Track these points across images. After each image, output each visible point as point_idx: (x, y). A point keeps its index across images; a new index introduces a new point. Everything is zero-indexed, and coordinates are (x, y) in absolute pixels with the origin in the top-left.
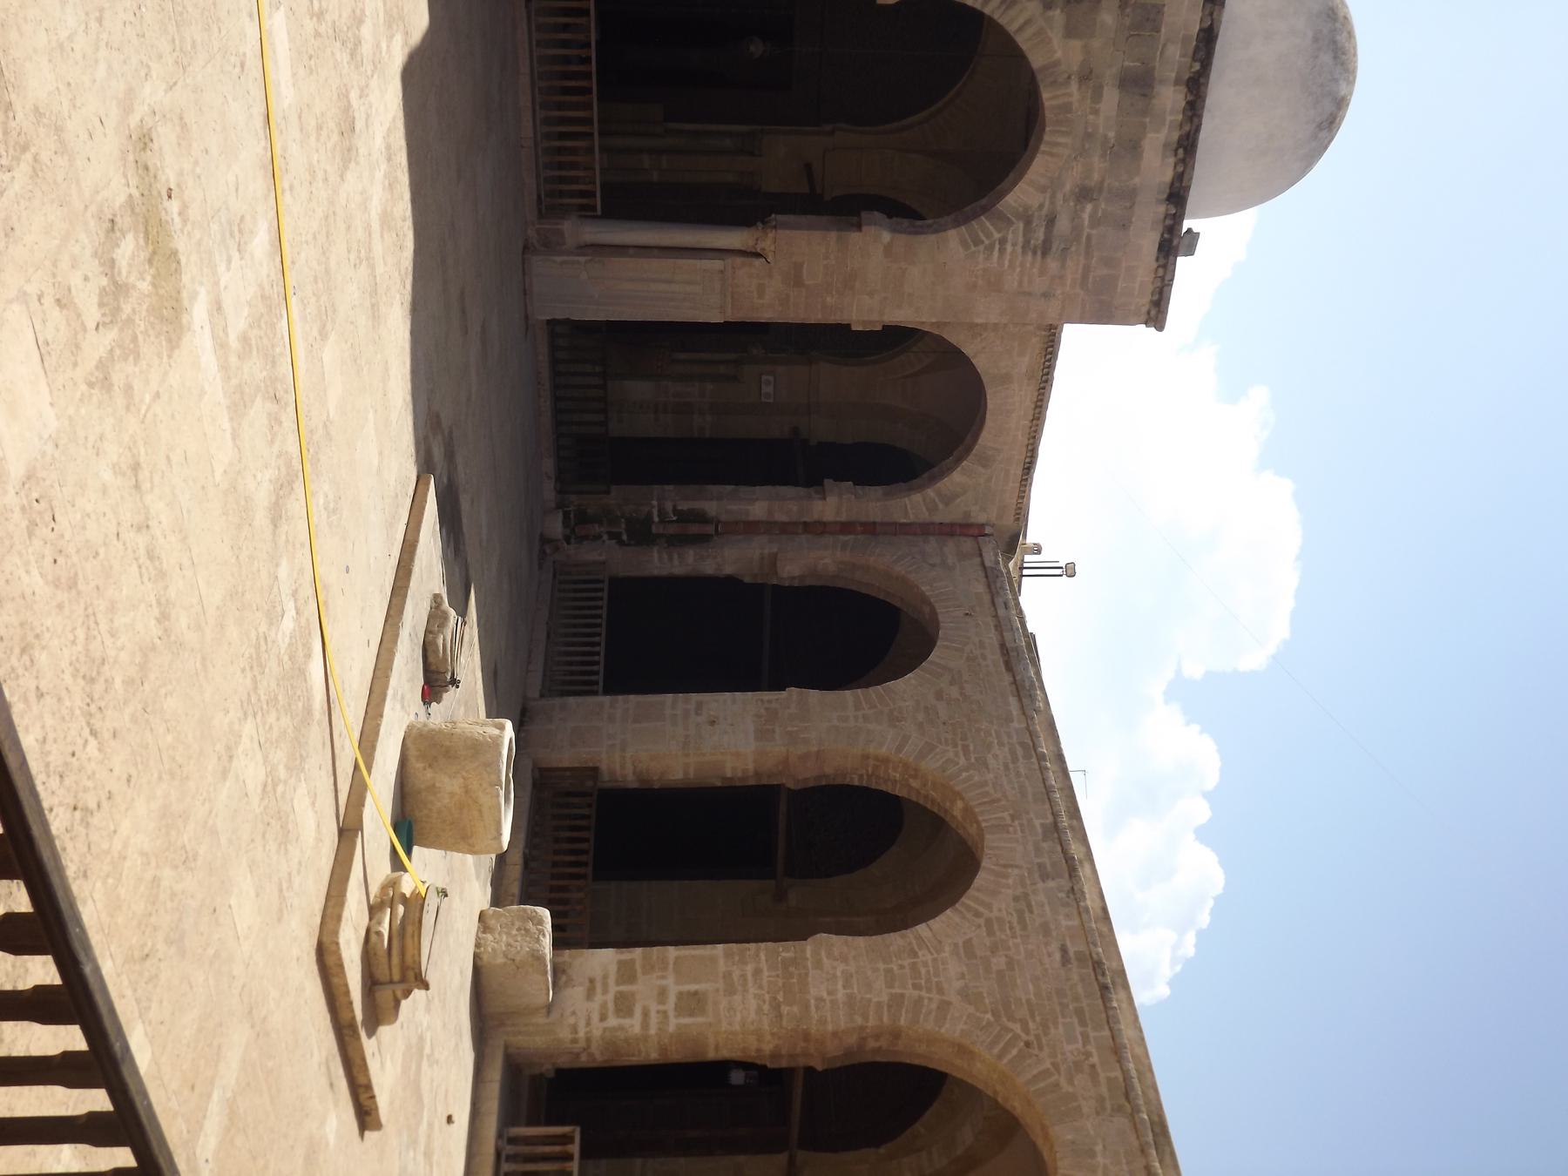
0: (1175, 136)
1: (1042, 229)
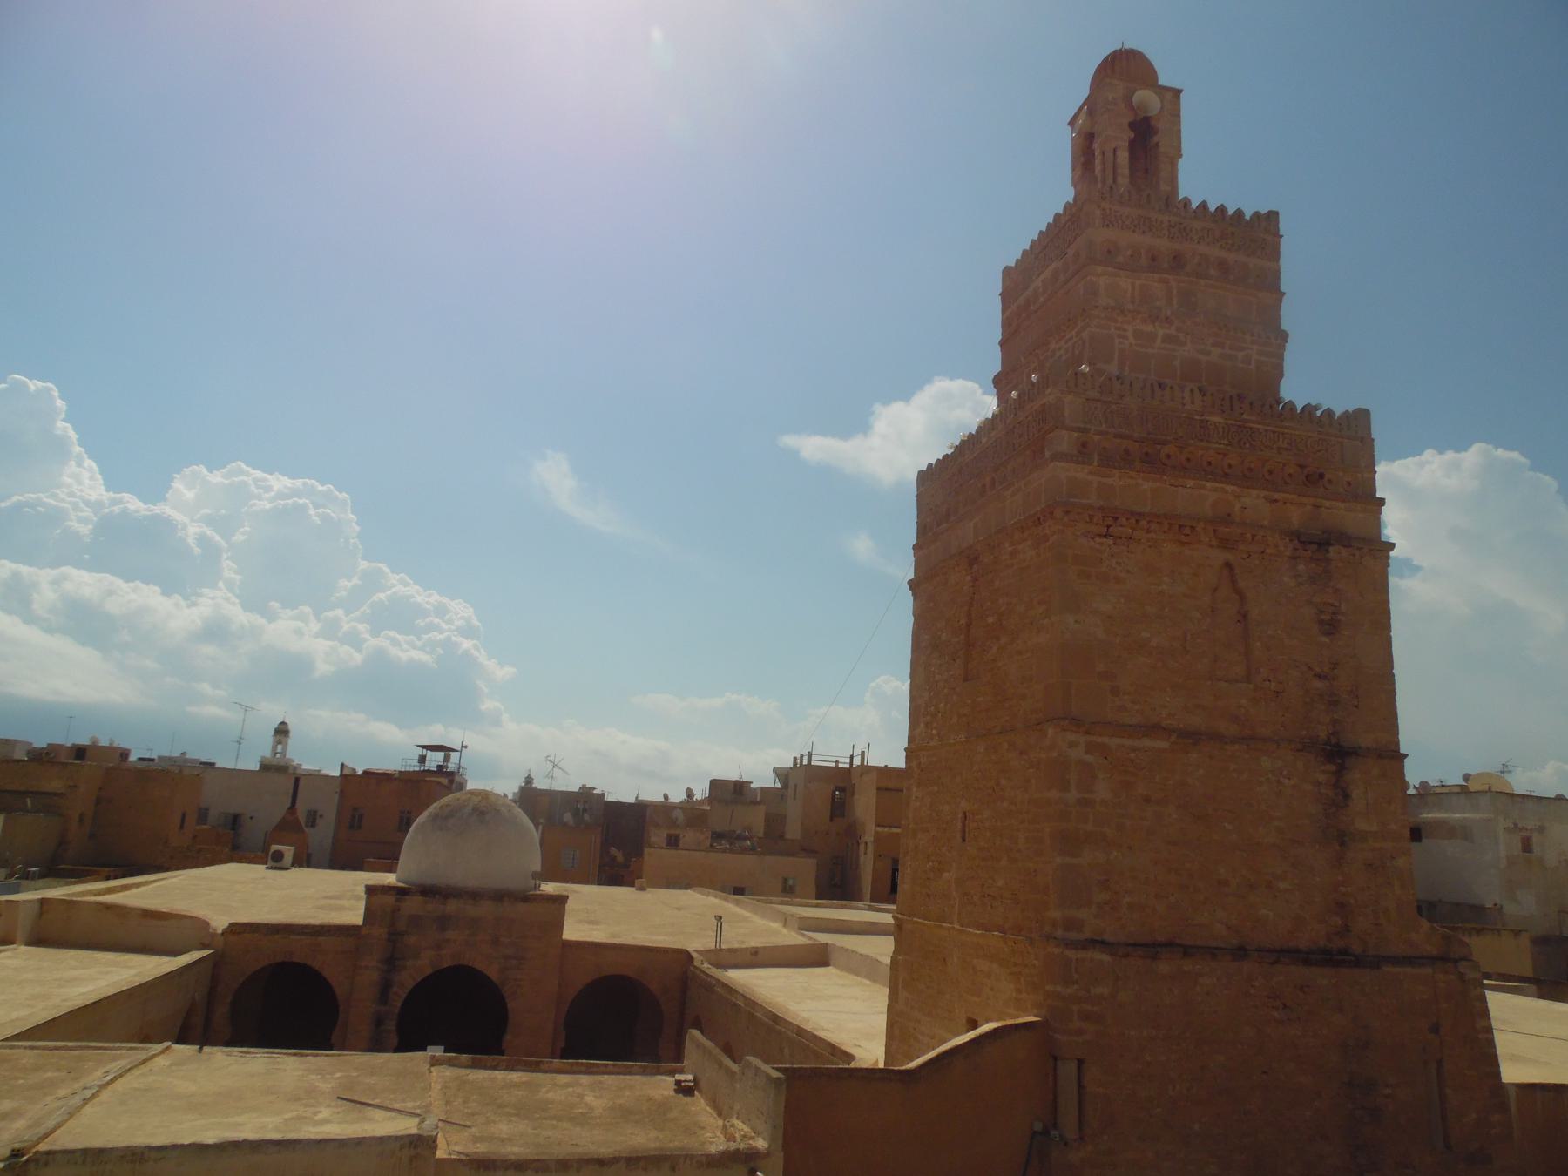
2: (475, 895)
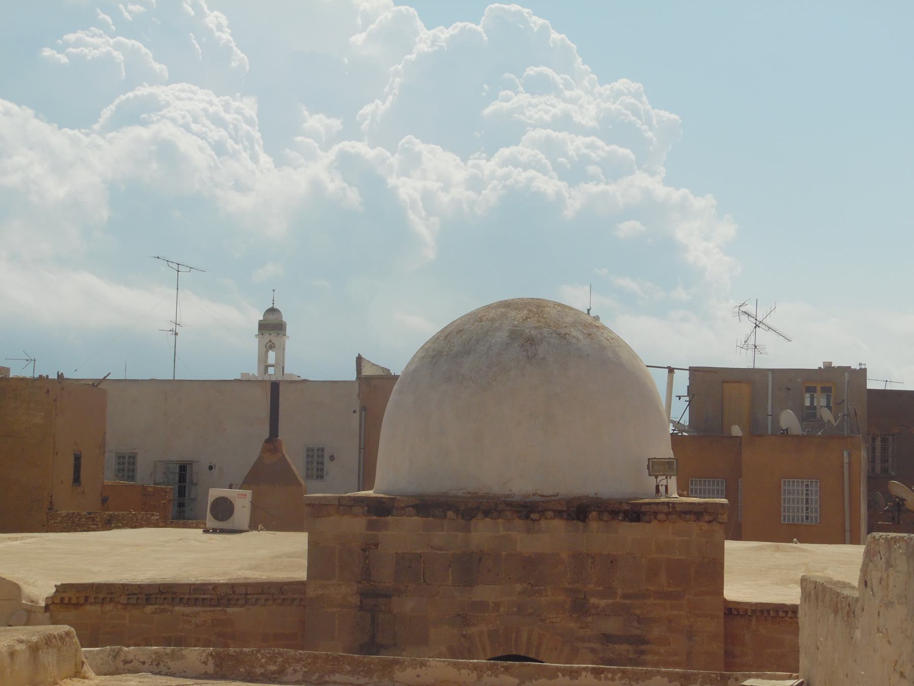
0: (519, 523)
1: (617, 647)
2: (528, 510)
